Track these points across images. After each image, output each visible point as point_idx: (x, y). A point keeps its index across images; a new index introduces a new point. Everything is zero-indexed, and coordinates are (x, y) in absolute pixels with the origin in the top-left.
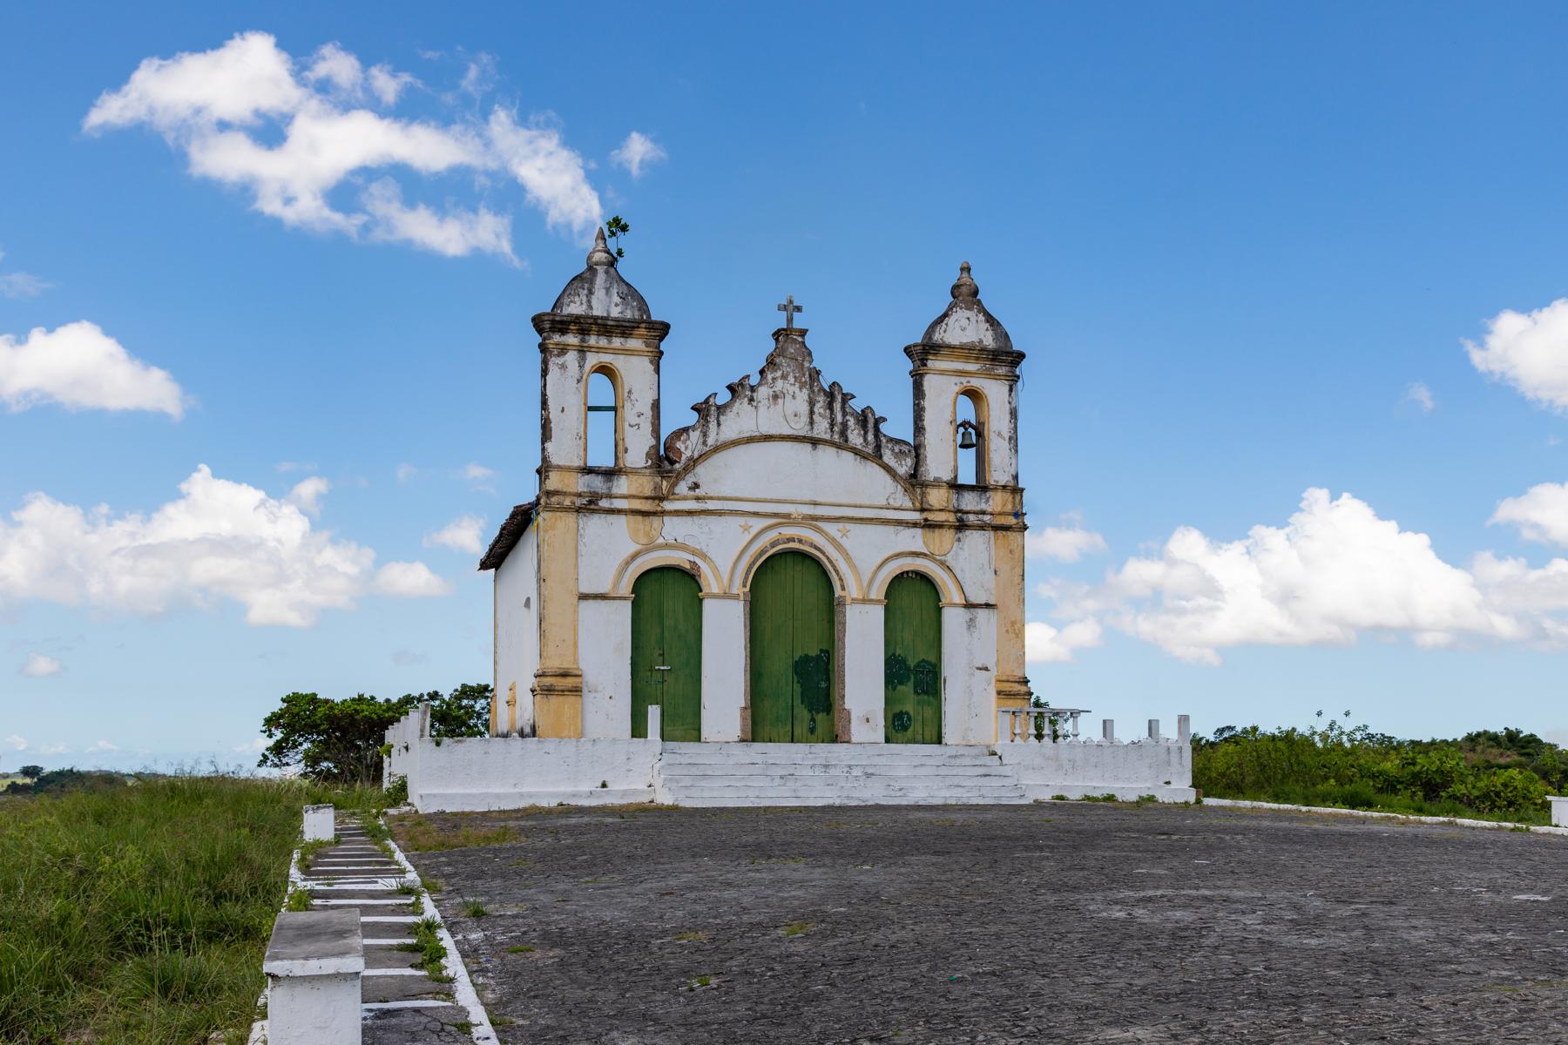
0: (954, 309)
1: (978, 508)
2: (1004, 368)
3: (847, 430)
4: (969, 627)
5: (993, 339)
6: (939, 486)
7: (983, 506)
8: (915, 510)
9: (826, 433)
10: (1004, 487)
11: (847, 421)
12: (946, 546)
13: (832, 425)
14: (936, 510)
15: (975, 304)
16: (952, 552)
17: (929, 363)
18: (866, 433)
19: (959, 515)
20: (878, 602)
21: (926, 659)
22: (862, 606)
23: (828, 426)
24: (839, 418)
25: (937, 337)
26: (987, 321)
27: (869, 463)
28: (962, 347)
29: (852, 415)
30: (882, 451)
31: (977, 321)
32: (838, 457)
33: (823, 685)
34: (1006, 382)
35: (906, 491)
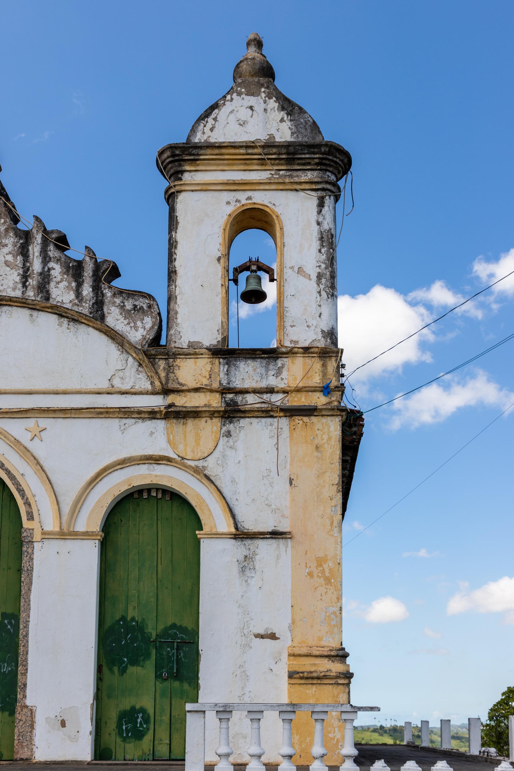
0: (229, 97)
1: (263, 384)
2: (309, 173)
3: (49, 283)
4: (243, 570)
5: (293, 134)
6: (195, 354)
7: (272, 381)
8: (154, 393)
9: (14, 289)
10: (306, 350)
11: (49, 269)
12: (207, 445)
13: (25, 277)
14: (189, 391)
15: (262, 85)
16: (216, 454)
17: (187, 177)
18: (80, 285)
19: (230, 396)
20: (87, 535)
21: (178, 624)
22: (62, 542)
23: (18, 279)
24: (37, 266)
25: (199, 138)
26: (283, 108)
27: (82, 328)
28: (233, 146)
29: (58, 260)
30: (105, 310)
31: (265, 110)
32: (33, 321)
33: (6, 669)
34: (313, 193)
35: (140, 365)
